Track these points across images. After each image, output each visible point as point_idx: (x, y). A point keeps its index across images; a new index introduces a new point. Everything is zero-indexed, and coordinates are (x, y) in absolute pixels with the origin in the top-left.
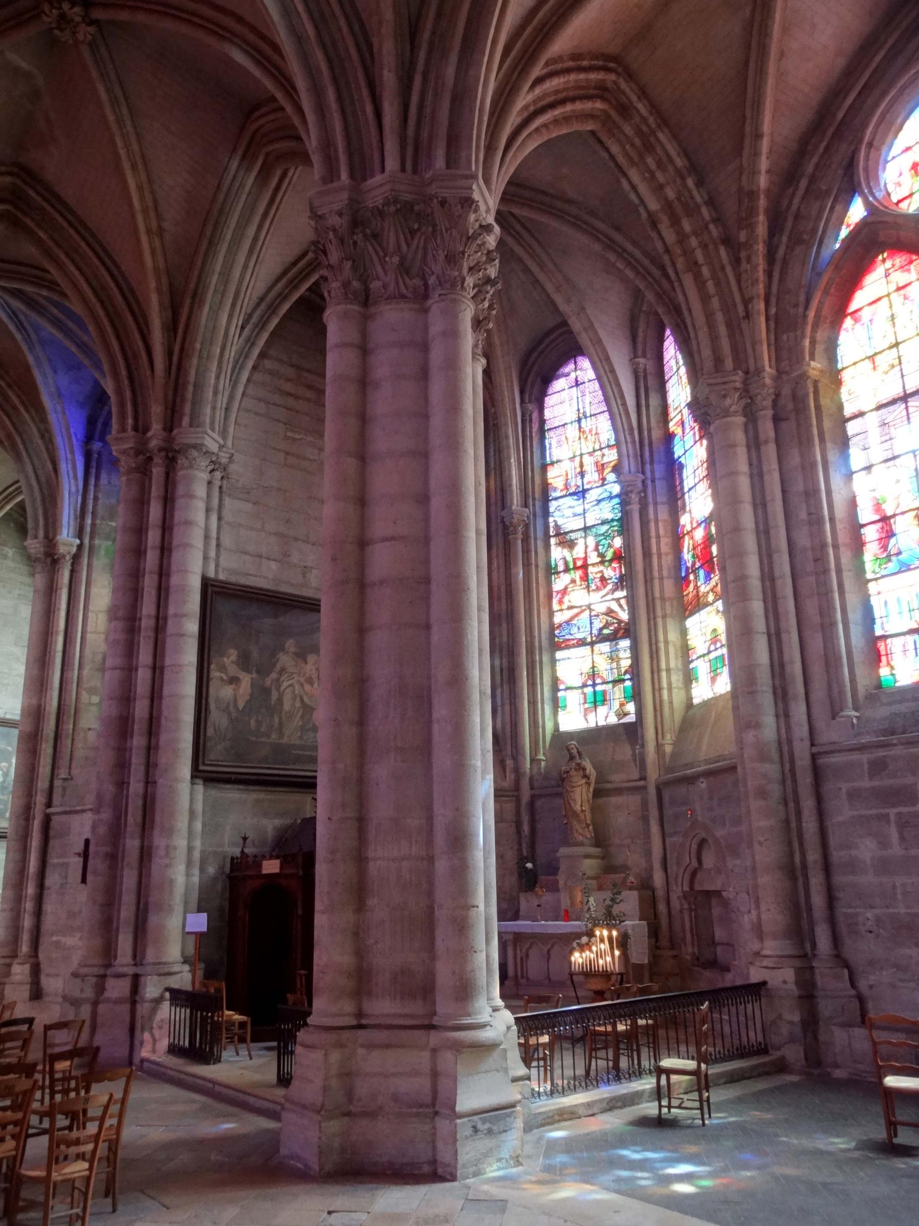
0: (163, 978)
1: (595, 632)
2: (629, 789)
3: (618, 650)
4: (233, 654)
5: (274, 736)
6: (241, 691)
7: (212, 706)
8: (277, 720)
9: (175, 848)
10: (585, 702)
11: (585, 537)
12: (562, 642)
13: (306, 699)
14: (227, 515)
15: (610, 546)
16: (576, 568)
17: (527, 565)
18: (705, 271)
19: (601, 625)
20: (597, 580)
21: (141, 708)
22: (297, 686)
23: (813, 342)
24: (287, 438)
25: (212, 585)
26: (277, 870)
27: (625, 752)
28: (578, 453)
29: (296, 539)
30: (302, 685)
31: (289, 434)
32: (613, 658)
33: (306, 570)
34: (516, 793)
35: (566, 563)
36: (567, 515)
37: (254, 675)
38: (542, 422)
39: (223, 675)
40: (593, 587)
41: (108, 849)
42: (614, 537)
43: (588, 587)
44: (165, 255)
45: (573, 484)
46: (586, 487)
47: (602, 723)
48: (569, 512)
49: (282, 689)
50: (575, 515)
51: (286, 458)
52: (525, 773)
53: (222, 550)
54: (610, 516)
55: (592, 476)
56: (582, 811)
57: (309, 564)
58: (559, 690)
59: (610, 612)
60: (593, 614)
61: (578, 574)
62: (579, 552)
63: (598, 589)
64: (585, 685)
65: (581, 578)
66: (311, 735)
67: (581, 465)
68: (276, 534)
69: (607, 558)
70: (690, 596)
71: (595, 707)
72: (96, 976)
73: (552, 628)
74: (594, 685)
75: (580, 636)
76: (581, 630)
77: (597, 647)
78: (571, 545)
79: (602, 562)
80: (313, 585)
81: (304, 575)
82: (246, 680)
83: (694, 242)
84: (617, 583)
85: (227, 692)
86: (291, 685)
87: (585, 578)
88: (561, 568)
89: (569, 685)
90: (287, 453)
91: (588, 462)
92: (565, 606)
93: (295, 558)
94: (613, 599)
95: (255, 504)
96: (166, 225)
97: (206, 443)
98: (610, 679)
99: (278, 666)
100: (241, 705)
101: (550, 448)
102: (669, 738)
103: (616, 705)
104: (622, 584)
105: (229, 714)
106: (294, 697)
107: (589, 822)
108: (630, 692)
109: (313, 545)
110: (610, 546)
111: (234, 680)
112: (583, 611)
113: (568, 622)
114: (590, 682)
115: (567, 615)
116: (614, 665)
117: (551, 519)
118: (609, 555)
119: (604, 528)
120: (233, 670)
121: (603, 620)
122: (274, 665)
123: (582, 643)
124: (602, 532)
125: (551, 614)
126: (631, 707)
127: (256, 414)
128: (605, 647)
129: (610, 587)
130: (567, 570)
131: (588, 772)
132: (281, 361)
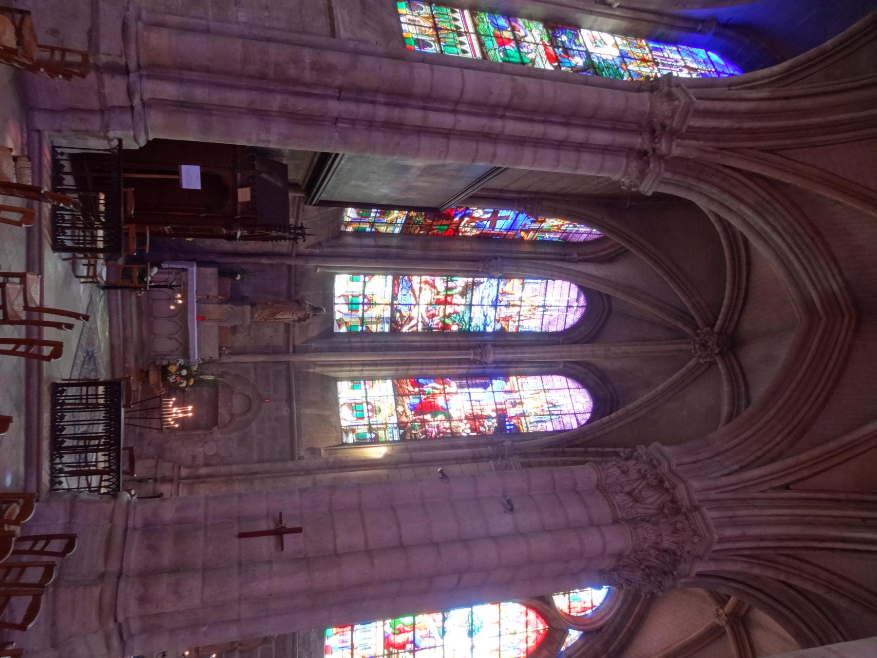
1: (400, 307)
2: (288, 339)
10: (353, 296)
11: (465, 305)
12: (398, 282)
15: (454, 322)
16: (447, 296)
20: (434, 311)
21: (414, 116)
26: (240, 200)
27: (314, 332)
28: (523, 304)
32: (379, 320)
34: (294, 255)
35: (452, 289)
36: (485, 291)
40: (430, 308)
41: (271, 74)
42: (459, 325)
45: (504, 298)
46: (498, 308)
47: (336, 308)
48: (486, 294)
50: (482, 298)
54: (473, 324)
55: (504, 312)
59: (410, 318)
60: (412, 306)
61: (442, 297)
62: (458, 299)
63: (428, 311)
64: (364, 296)
65: (438, 300)
67: (514, 306)
69: (446, 320)
70: (406, 387)
71: (348, 304)
72: (127, 65)
74: (363, 304)
75: (399, 296)
76: (403, 297)
77: (389, 307)
78: (463, 294)
79: (445, 316)
87: (438, 302)
88: (450, 284)
89: (367, 285)
91: (513, 311)
92: (423, 286)
94: (418, 322)
101: (534, 283)
102: (318, 370)
103: (347, 319)
104: (427, 329)
108: (354, 329)
112: (416, 299)
113: (411, 287)
114: (366, 301)
115: (416, 287)
116: (374, 320)
117: (485, 279)
118: (448, 321)
119: (467, 319)
123: (394, 296)
126: (343, 329)
129: (427, 320)
130: (447, 289)
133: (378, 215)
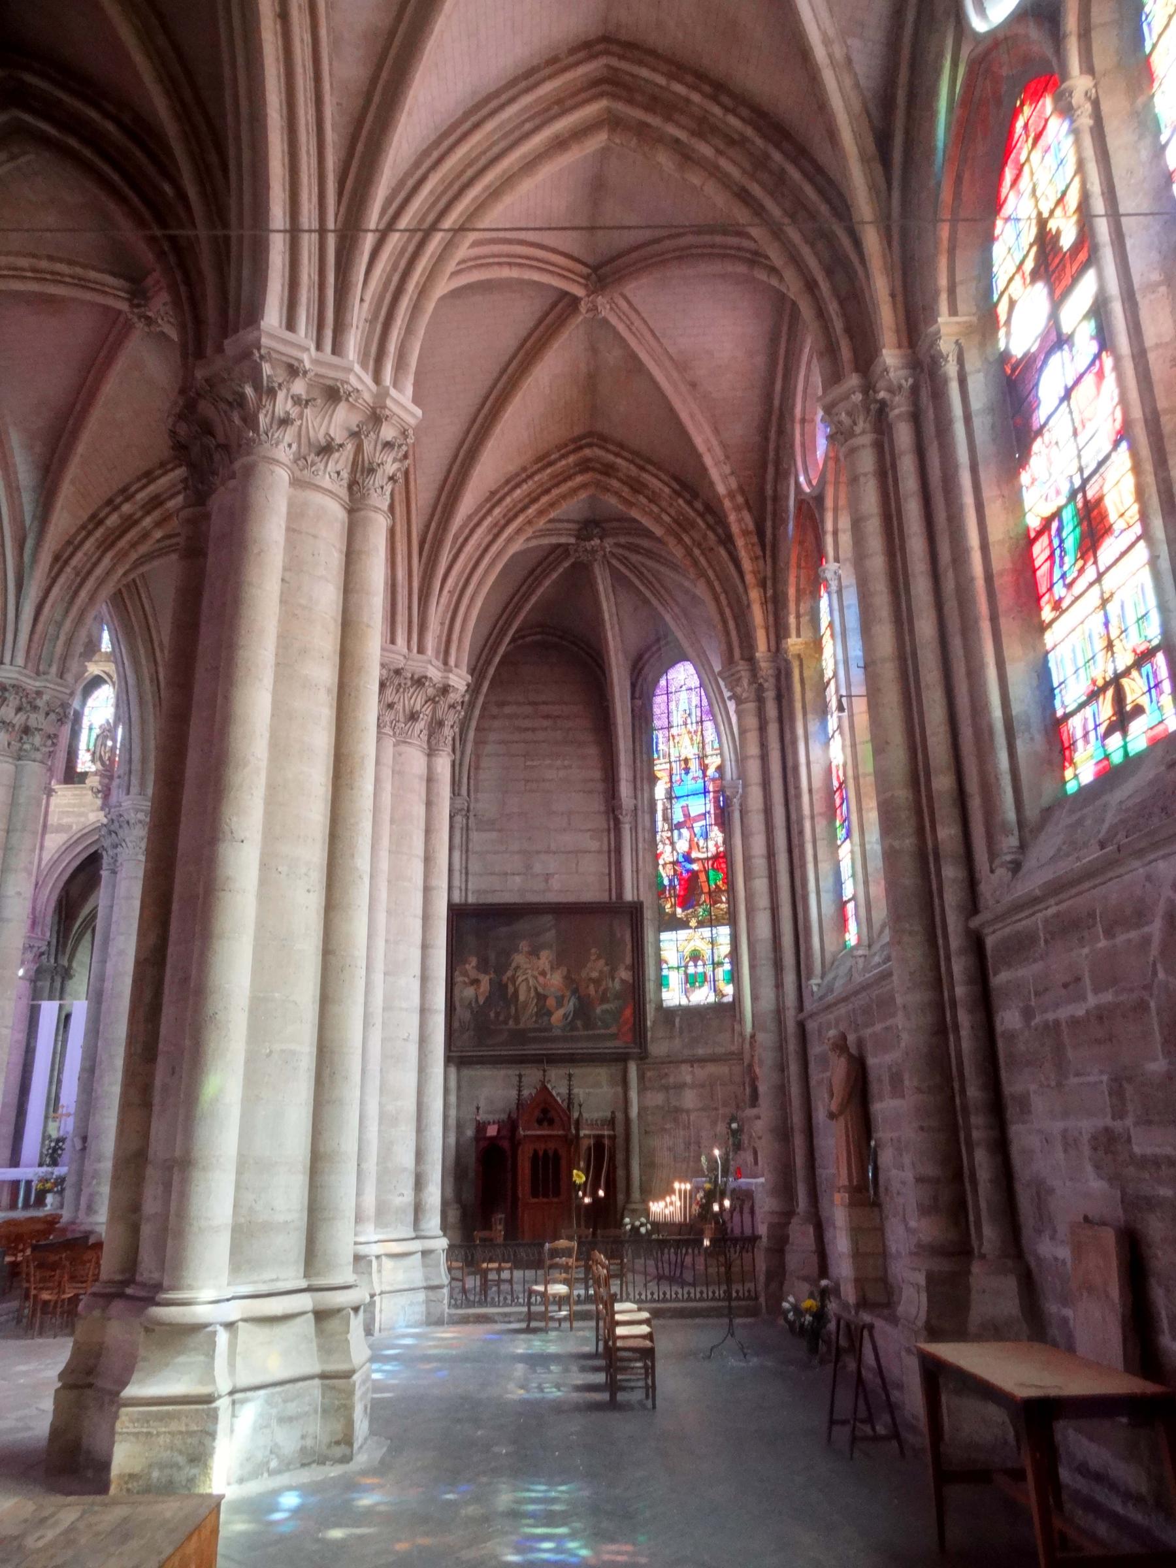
4: (474, 961)
5: (511, 1022)
6: (482, 989)
7: (457, 1004)
13: (540, 990)
14: (475, 846)
18: (710, 573)
23: (798, 617)
24: (526, 767)
29: (538, 852)
30: (536, 978)
31: (529, 763)
33: (547, 877)
37: (492, 976)
39: (466, 980)
57: (551, 871)
66: (546, 1018)
68: (519, 852)
82: (485, 980)
83: (697, 552)
85: (469, 992)
93: (538, 868)
95: (500, 831)
99: (514, 965)
100: (481, 1000)
105: (472, 1009)
109: (554, 853)
111: (475, 982)
120: (473, 974)
127: (498, 755)
132: (518, 704)
133: (700, 963)
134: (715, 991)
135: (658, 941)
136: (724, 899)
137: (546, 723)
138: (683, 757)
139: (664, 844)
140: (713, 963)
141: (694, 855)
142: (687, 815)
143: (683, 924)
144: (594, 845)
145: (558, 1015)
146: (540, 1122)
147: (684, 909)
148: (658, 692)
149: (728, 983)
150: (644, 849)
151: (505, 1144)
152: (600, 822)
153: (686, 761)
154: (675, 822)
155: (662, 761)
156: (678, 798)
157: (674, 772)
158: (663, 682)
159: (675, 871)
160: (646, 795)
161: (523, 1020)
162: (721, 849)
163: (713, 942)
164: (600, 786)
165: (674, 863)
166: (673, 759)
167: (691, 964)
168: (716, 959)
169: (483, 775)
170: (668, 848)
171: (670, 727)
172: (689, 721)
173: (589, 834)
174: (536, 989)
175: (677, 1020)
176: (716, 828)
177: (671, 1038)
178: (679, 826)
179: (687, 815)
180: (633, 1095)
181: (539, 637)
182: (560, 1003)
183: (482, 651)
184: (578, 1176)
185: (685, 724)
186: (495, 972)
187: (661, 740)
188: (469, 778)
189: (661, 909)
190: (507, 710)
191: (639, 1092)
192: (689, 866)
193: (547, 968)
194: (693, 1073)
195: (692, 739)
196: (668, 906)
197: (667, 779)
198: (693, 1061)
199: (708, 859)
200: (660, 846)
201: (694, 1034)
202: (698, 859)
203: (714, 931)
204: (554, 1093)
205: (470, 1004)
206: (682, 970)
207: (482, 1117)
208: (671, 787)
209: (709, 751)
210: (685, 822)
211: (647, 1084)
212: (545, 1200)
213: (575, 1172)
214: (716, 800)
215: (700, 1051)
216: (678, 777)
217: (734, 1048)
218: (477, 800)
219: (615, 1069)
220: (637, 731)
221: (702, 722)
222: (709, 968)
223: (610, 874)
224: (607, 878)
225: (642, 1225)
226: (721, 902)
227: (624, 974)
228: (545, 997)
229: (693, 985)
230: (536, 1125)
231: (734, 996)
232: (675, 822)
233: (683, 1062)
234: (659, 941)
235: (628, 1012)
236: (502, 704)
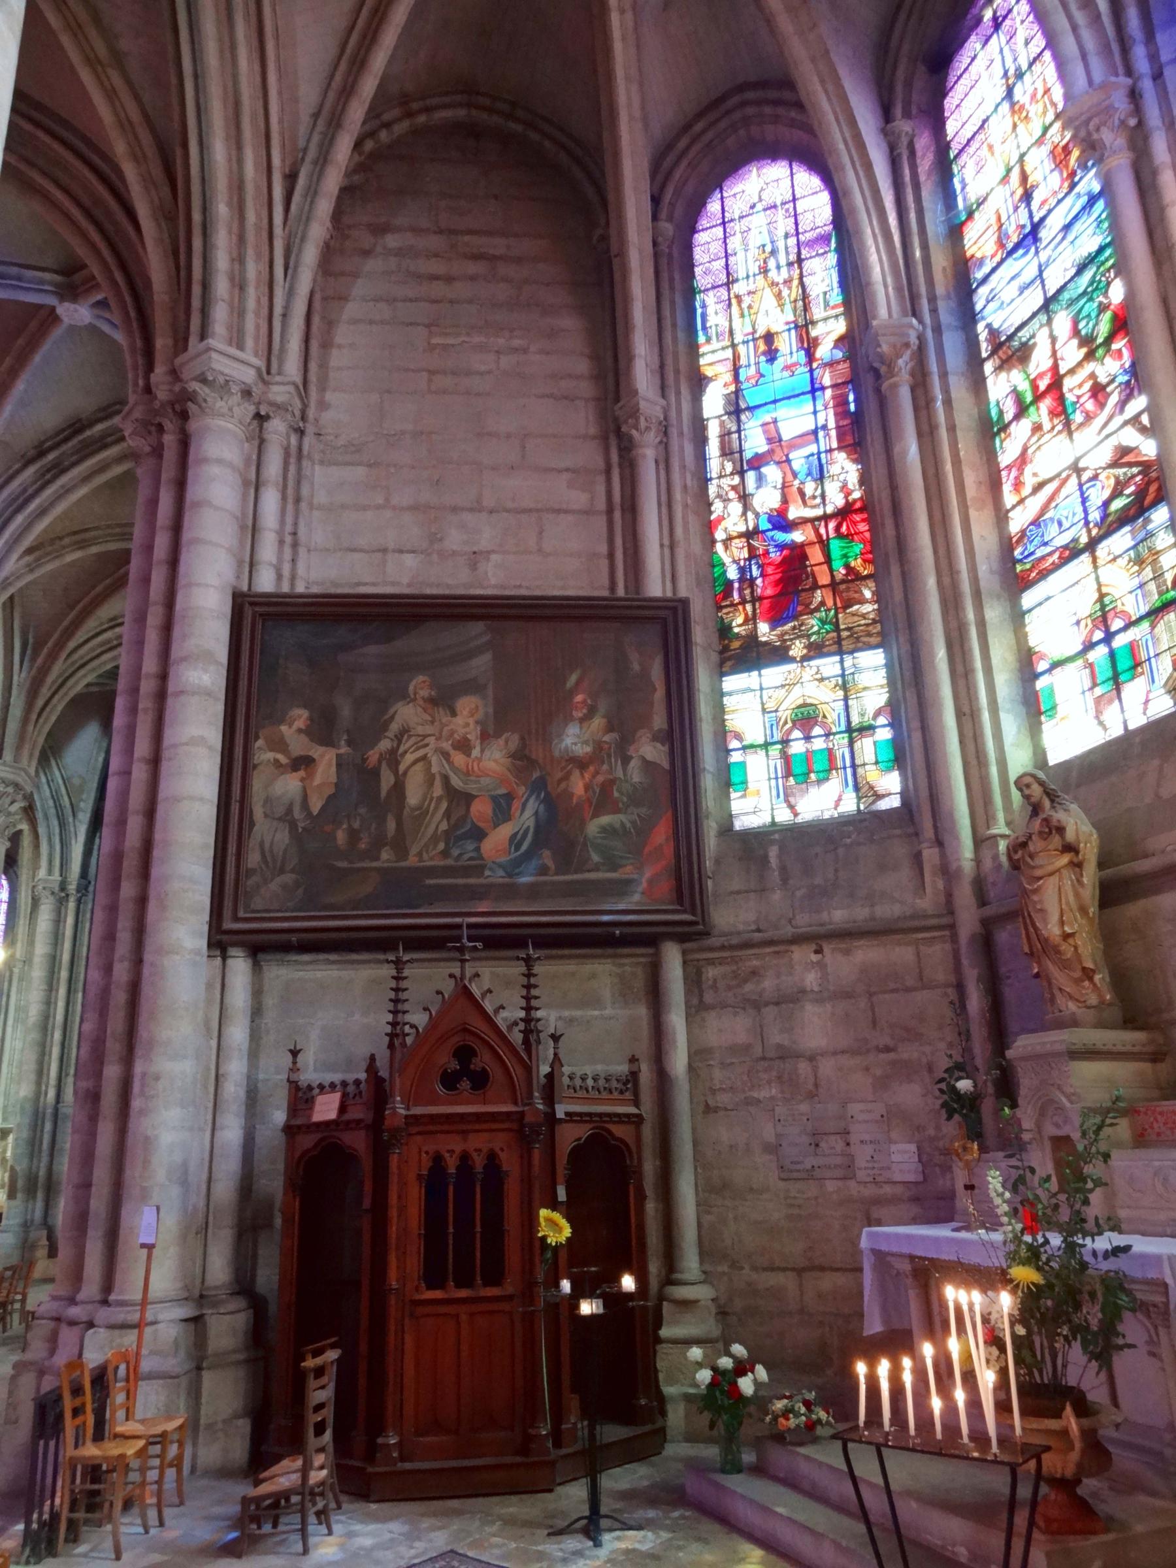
0: (117, 1332)
1: (1095, 516)
3: (1150, 535)
4: (300, 717)
5: (386, 855)
7: (258, 812)
8: (391, 825)
9: (157, 1078)
10: (1095, 685)
11: (1049, 321)
13: (456, 782)
15: (1102, 308)
16: (1038, 397)
17: (927, 433)
19: (1106, 494)
22: (434, 760)
24: (432, 348)
25: (252, 604)
29: (455, 509)
30: (446, 755)
33: (475, 558)
37: (344, 750)
38: (942, 147)
40: (1078, 417)
42: (1108, 284)
43: (1068, 424)
44: (137, 97)
47: (1137, 721)
49: (402, 768)
51: (430, 381)
52: (959, 869)
53: (302, 551)
56: (1066, 936)
57: (484, 544)
58: (1037, 676)
59: (1122, 455)
64: (1089, 646)
65: (1053, 414)
66: (470, 846)
68: (414, 508)
69: (1100, 340)
73: (1007, 545)
74: (1109, 637)
75: (1063, 540)
76: (1066, 525)
77: (1102, 550)
79: (1090, 356)
80: (493, 581)
81: (473, 566)
82: (326, 761)
84: (1128, 383)
85: (289, 785)
86: (424, 758)
87: (1060, 410)
90: (432, 373)
93: (454, 539)
94: (1126, 423)
95: (370, 466)
96: (124, 44)
97: (215, 366)
98: (1144, 609)
99: (394, 727)
100: (316, 805)
105: (293, 825)
106: (430, 780)
107: (1089, 965)
110: (1102, 308)
111: (303, 763)
112: (1064, 482)
113: (1035, 523)
115: (1034, 505)
117: (981, 327)
120: (299, 745)
121: (1107, 483)
122: (385, 727)
123: (1071, 553)
124: (1081, 290)
125: (1001, 516)
128: (1122, 540)
129: (1114, 399)
130: (1022, 410)
131: (1070, 835)
132: (416, 230)
133: (817, 731)
134: (857, 788)
135: (719, 694)
136: (868, 594)
137: (473, 268)
138: (761, 331)
139: (726, 500)
140: (849, 730)
141: (795, 512)
142: (775, 440)
143: (778, 654)
144: (579, 499)
145: (497, 840)
146: (450, 1081)
147: (775, 622)
148: (703, 223)
149: (889, 770)
150: (686, 506)
151: (357, 1141)
152: (589, 455)
153: (769, 337)
154: (748, 455)
155: (715, 345)
156: (751, 409)
157: (743, 361)
158: (714, 206)
159: (751, 549)
160: (686, 407)
161: (414, 851)
162: (857, 495)
163: (845, 686)
164: (587, 389)
165: (748, 535)
166: (738, 338)
167: (797, 734)
168: (855, 720)
169: (337, 358)
170: (736, 507)
171: (730, 282)
172: (772, 264)
173: (566, 476)
174: (446, 779)
175: (773, 852)
176: (841, 457)
177: (762, 890)
178: (757, 463)
179: (775, 440)
180: (677, 1020)
181: (461, 113)
182: (503, 808)
183: (336, 66)
184: (551, 1222)
185: (764, 271)
186: (349, 743)
187: (710, 311)
188: (307, 340)
189: (724, 631)
190: (392, 241)
191: (689, 1018)
192: (781, 537)
193: (473, 735)
194: (821, 965)
195: (779, 296)
196: (740, 620)
197: (729, 377)
198: (817, 939)
199: (826, 518)
200: (717, 507)
201: (818, 881)
202: (805, 521)
203: (848, 661)
204: (489, 1006)
205: (289, 810)
206: (775, 751)
207: (309, 1076)
208: (737, 393)
209: (817, 312)
210: (771, 452)
211: (709, 997)
212: (463, 1293)
213: (544, 1213)
214: (840, 403)
215: (838, 916)
216: (752, 371)
217: (926, 903)
218: (323, 405)
219: (632, 964)
220: (665, 285)
221: (800, 261)
222: (841, 740)
223: (611, 556)
224: (604, 564)
225: (741, 1369)
226: (862, 601)
227: (650, 750)
228: (468, 798)
229: (805, 779)
230: (440, 1089)
231: (904, 794)
232: (748, 455)
233: (798, 940)
234: (722, 694)
235: (661, 835)
236: (380, 230)
